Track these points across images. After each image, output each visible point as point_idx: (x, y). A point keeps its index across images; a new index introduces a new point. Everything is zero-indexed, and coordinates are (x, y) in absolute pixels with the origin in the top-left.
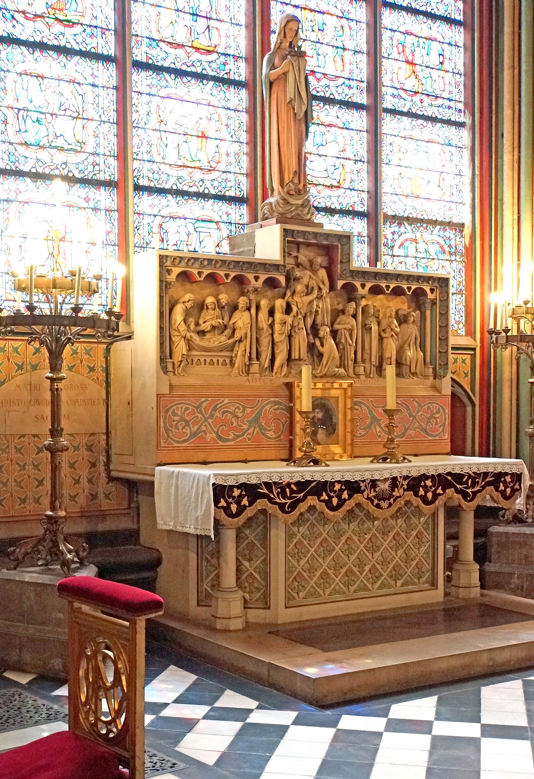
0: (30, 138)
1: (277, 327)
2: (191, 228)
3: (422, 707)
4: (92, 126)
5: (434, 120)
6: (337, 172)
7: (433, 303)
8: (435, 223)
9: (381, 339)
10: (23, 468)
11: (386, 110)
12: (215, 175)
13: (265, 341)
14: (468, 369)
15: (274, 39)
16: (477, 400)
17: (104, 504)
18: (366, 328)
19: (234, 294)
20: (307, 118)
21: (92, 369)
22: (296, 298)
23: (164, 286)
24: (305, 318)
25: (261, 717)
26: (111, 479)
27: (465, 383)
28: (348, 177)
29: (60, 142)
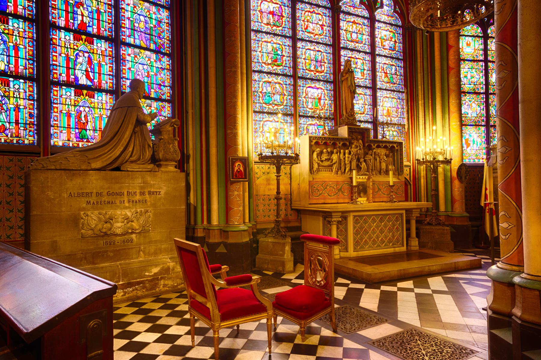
0: (266, 101)
1: (346, 159)
2: (316, 128)
3: (409, 284)
4: (285, 97)
7: (397, 150)
9: (380, 162)
10: (264, 205)
11: (378, 89)
13: (343, 164)
14: (408, 173)
15: (342, 67)
16: (412, 183)
17: (290, 217)
18: (375, 159)
19: (332, 149)
20: (354, 92)
21: (286, 174)
22: (352, 149)
23: (311, 146)
25: (352, 286)
26: (292, 209)
27: (408, 177)
29: (275, 103)
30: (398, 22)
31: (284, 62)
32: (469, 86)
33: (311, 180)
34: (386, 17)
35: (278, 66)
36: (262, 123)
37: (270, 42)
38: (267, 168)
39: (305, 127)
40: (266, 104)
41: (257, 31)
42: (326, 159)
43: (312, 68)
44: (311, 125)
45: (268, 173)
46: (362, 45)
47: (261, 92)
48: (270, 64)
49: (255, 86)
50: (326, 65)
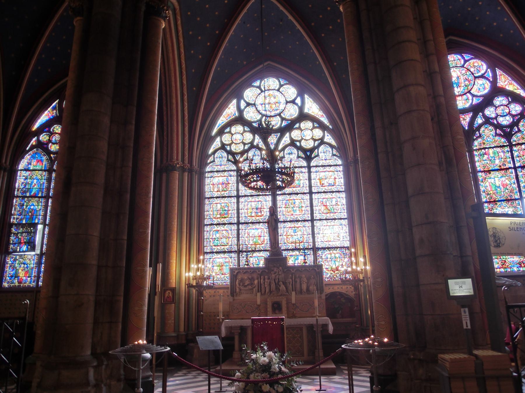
4: (230, 239)
5: (335, 219)
8: (337, 248)
12: (263, 245)
13: (262, 287)
24: (275, 280)
28: (305, 239)
30: (336, 161)
33: (231, 300)
34: (324, 161)
35: (225, 218)
38: (213, 292)
42: (248, 285)
43: (253, 214)
45: (214, 296)
50: (265, 210)
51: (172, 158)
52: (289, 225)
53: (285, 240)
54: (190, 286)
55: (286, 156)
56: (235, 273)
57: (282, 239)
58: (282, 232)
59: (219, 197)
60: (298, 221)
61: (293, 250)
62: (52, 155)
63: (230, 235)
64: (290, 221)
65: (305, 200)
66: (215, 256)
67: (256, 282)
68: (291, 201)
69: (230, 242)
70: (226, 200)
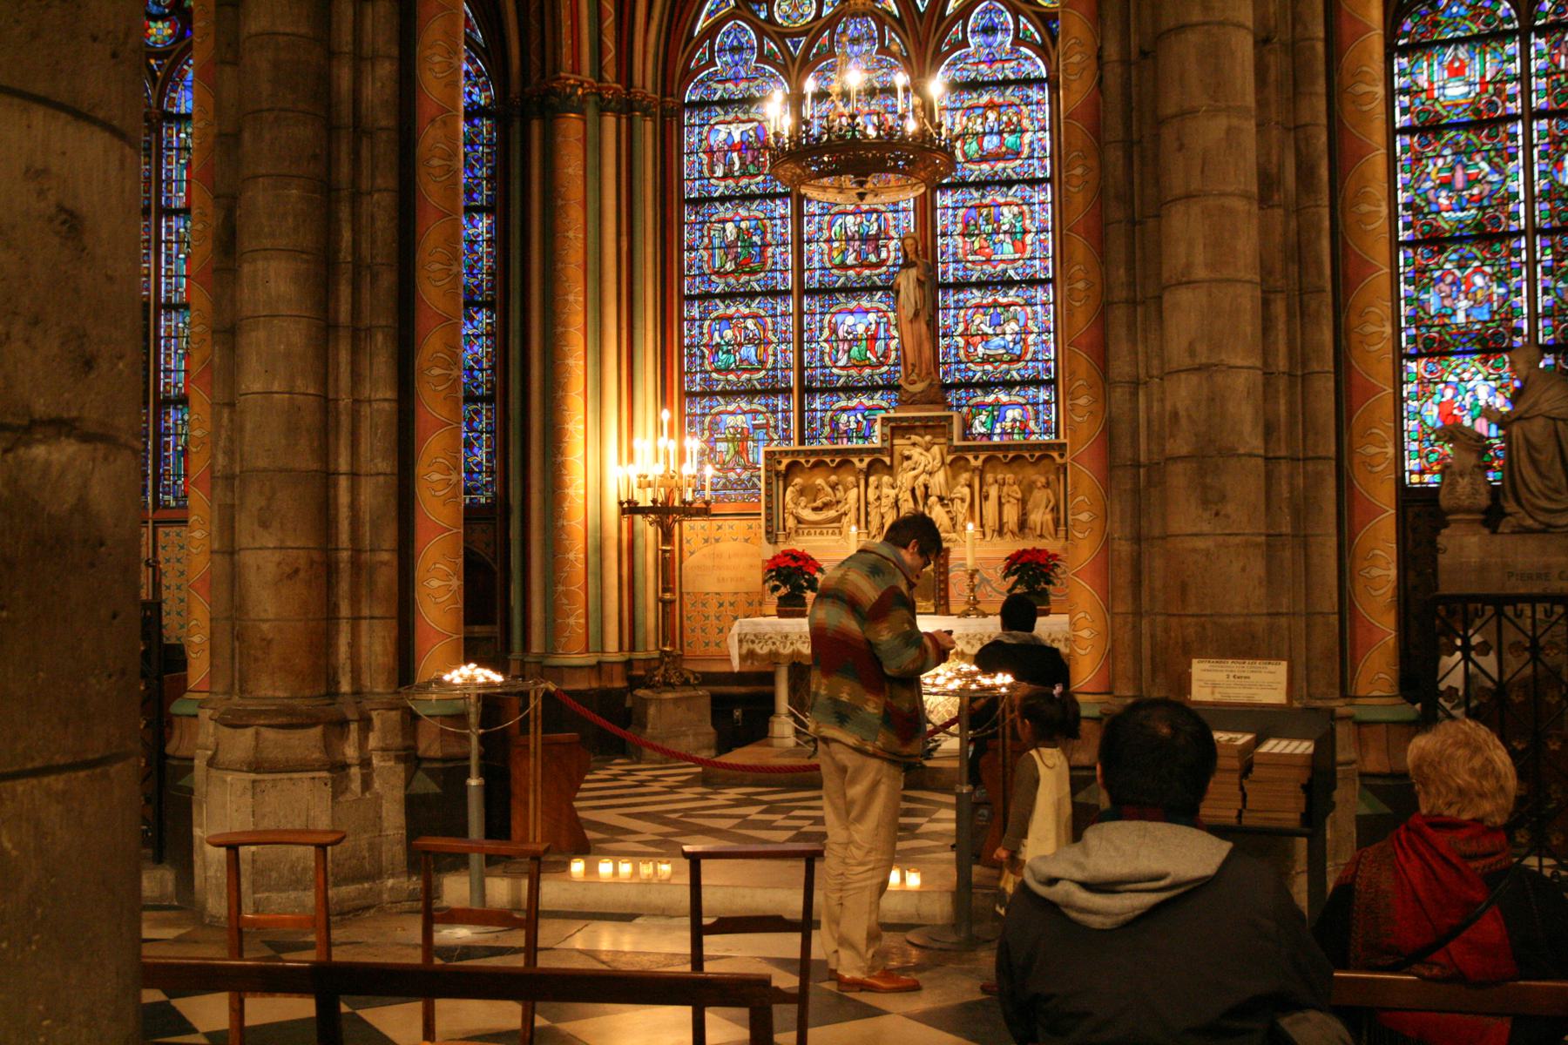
2: (859, 417)
6: (1018, 347)
9: (1000, 505)
28: (1032, 349)
31: (770, 261)
32: (1460, 214)
35: (753, 272)
36: (708, 419)
37: (731, 220)
39: (827, 420)
40: (718, 371)
41: (697, 202)
43: (850, 260)
44: (843, 410)
46: (1019, 162)
47: (706, 345)
48: (732, 272)
49: (690, 333)
51: (556, 68)
52: (975, 296)
53: (962, 352)
54: (630, 509)
55: (974, 41)
56: (782, 467)
57: (949, 346)
58: (950, 321)
59: (730, 198)
60: (1010, 283)
61: (987, 386)
62: (152, 62)
63: (770, 334)
64: (980, 285)
65: (1037, 207)
66: (721, 405)
67: (853, 494)
68: (985, 211)
69: (771, 359)
70: (756, 209)
